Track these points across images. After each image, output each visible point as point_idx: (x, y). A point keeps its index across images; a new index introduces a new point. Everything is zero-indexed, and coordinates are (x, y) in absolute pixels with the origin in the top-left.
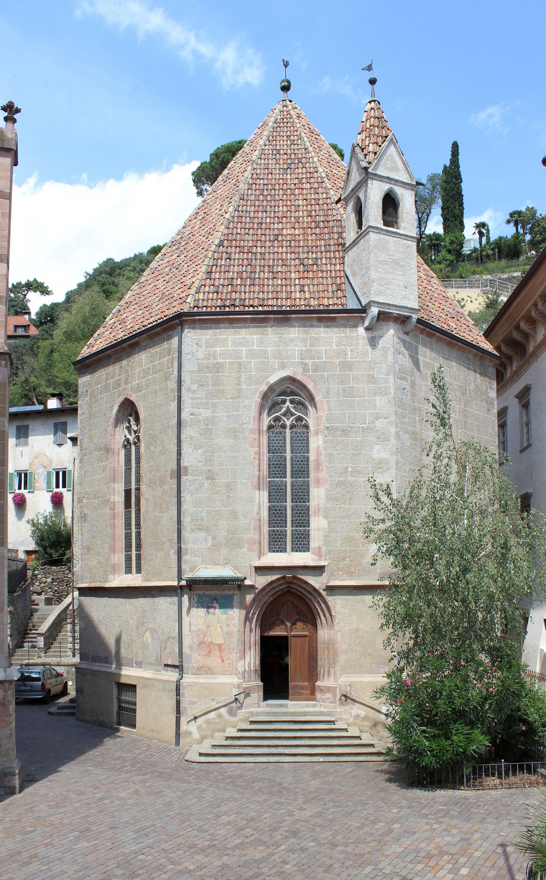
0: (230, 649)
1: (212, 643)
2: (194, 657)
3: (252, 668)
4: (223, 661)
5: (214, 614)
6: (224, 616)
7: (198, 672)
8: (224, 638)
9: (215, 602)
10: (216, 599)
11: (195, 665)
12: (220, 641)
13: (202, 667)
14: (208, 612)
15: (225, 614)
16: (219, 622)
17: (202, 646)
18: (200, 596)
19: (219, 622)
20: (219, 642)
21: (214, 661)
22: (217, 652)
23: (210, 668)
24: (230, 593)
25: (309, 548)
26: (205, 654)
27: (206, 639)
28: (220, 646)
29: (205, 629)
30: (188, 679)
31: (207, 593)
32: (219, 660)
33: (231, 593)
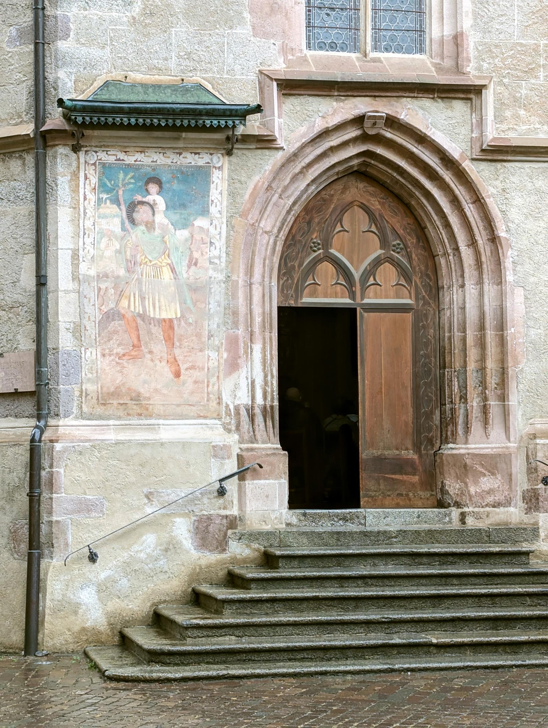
0: (199, 336)
1: (143, 316)
2: (87, 362)
3: (259, 400)
4: (177, 374)
5: (150, 226)
6: (183, 234)
7: (99, 410)
8: (183, 302)
9: (153, 188)
10: (158, 182)
11: (90, 387)
12: (170, 312)
13: (116, 394)
14: (133, 221)
15: (185, 226)
16: (166, 252)
17: (115, 324)
18: (106, 169)
19: (166, 252)
20: (164, 315)
21: (149, 376)
22: (160, 348)
23: (137, 398)
24: (201, 163)
25: (422, 42)
26: (120, 350)
27: (124, 303)
28: (168, 325)
29: (122, 272)
30: (70, 429)
31: (130, 159)
32: (167, 372)
33: (201, 160)
